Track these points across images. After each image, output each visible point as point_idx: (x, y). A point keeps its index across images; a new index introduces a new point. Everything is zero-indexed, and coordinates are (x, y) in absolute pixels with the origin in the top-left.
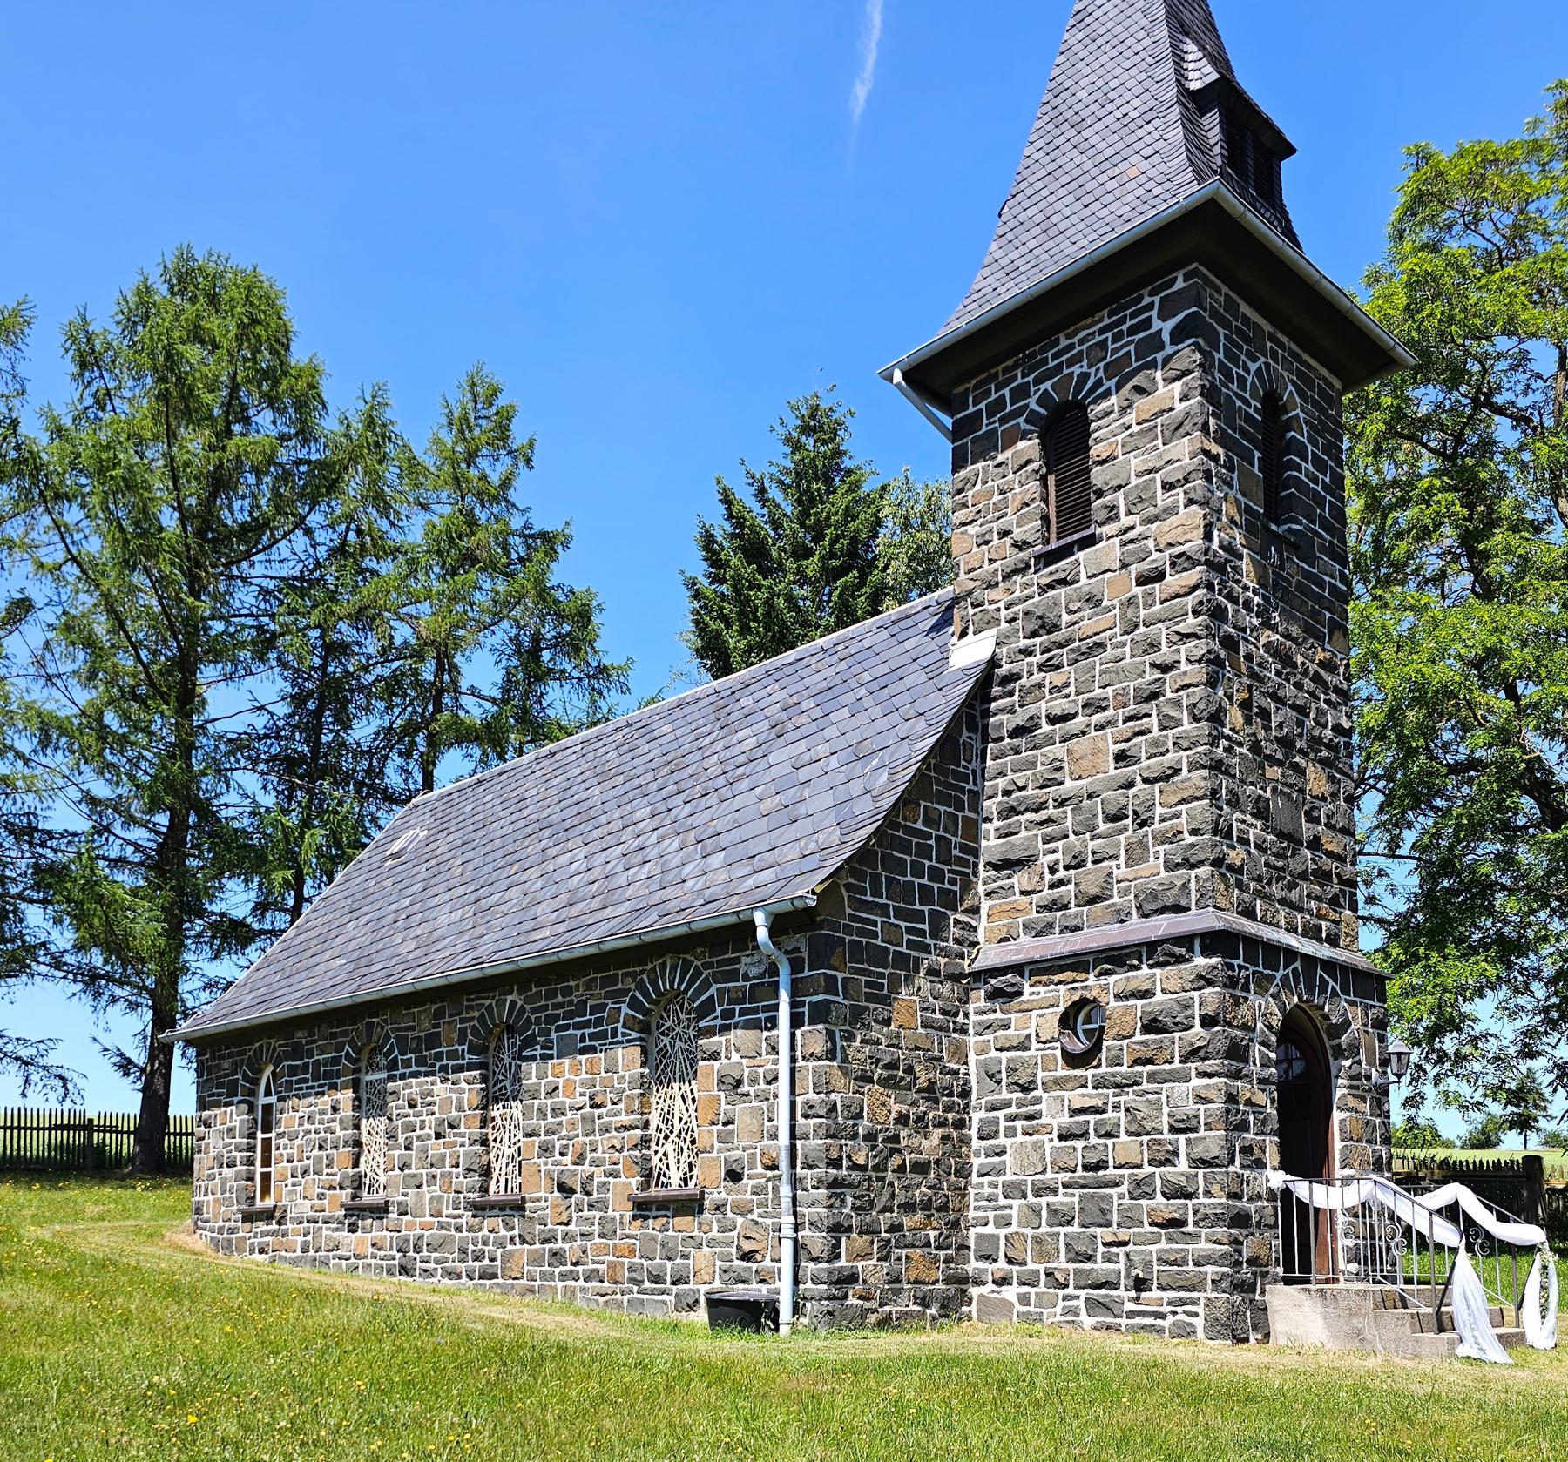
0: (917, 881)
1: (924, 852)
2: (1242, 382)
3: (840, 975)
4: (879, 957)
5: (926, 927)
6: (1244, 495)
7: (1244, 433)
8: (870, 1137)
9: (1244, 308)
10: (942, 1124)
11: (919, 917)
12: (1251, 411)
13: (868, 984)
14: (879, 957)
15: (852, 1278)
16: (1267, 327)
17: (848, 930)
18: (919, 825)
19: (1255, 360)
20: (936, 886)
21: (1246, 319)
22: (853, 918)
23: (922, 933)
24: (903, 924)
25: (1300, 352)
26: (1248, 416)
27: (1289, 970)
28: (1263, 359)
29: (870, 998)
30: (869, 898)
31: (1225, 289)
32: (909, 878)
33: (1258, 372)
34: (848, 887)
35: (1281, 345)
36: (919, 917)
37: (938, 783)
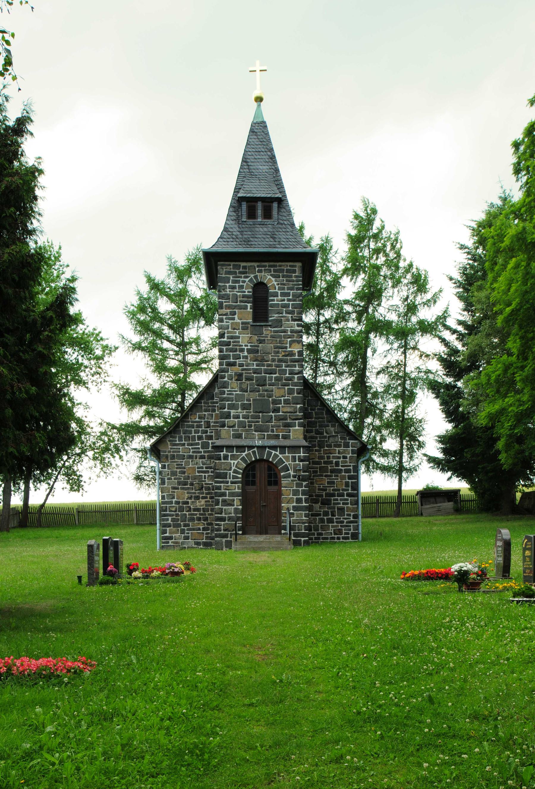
0: (196, 435)
1: (200, 426)
2: (241, 287)
3: (167, 464)
4: (183, 457)
5: (200, 446)
6: (241, 319)
7: (241, 301)
8: (177, 503)
9: (243, 264)
10: (206, 498)
11: (198, 444)
12: (246, 293)
13: (177, 465)
14: (183, 457)
15: (171, 538)
16: (256, 264)
17: (169, 452)
18: (197, 420)
19: (247, 277)
20: (204, 435)
21: (244, 267)
22: (171, 449)
23: (199, 448)
24: (190, 447)
25: (275, 264)
26: (244, 296)
27: (250, 451)
28: (252, 276)
29: (177, 468)
30: (178, 442)
31: (232, 263)
32: (193, 434)
33: (251, 281)
34: (169, 441)
35: (265, 266)
36: (198, 444)
37: (205, 406)
